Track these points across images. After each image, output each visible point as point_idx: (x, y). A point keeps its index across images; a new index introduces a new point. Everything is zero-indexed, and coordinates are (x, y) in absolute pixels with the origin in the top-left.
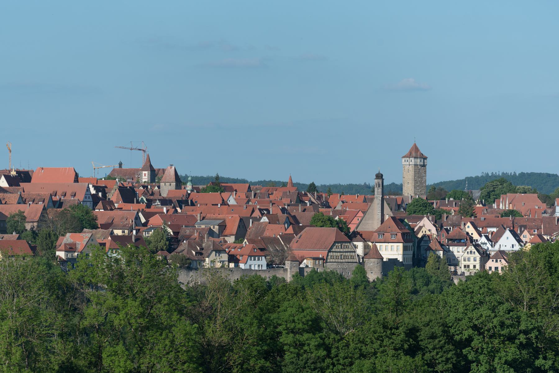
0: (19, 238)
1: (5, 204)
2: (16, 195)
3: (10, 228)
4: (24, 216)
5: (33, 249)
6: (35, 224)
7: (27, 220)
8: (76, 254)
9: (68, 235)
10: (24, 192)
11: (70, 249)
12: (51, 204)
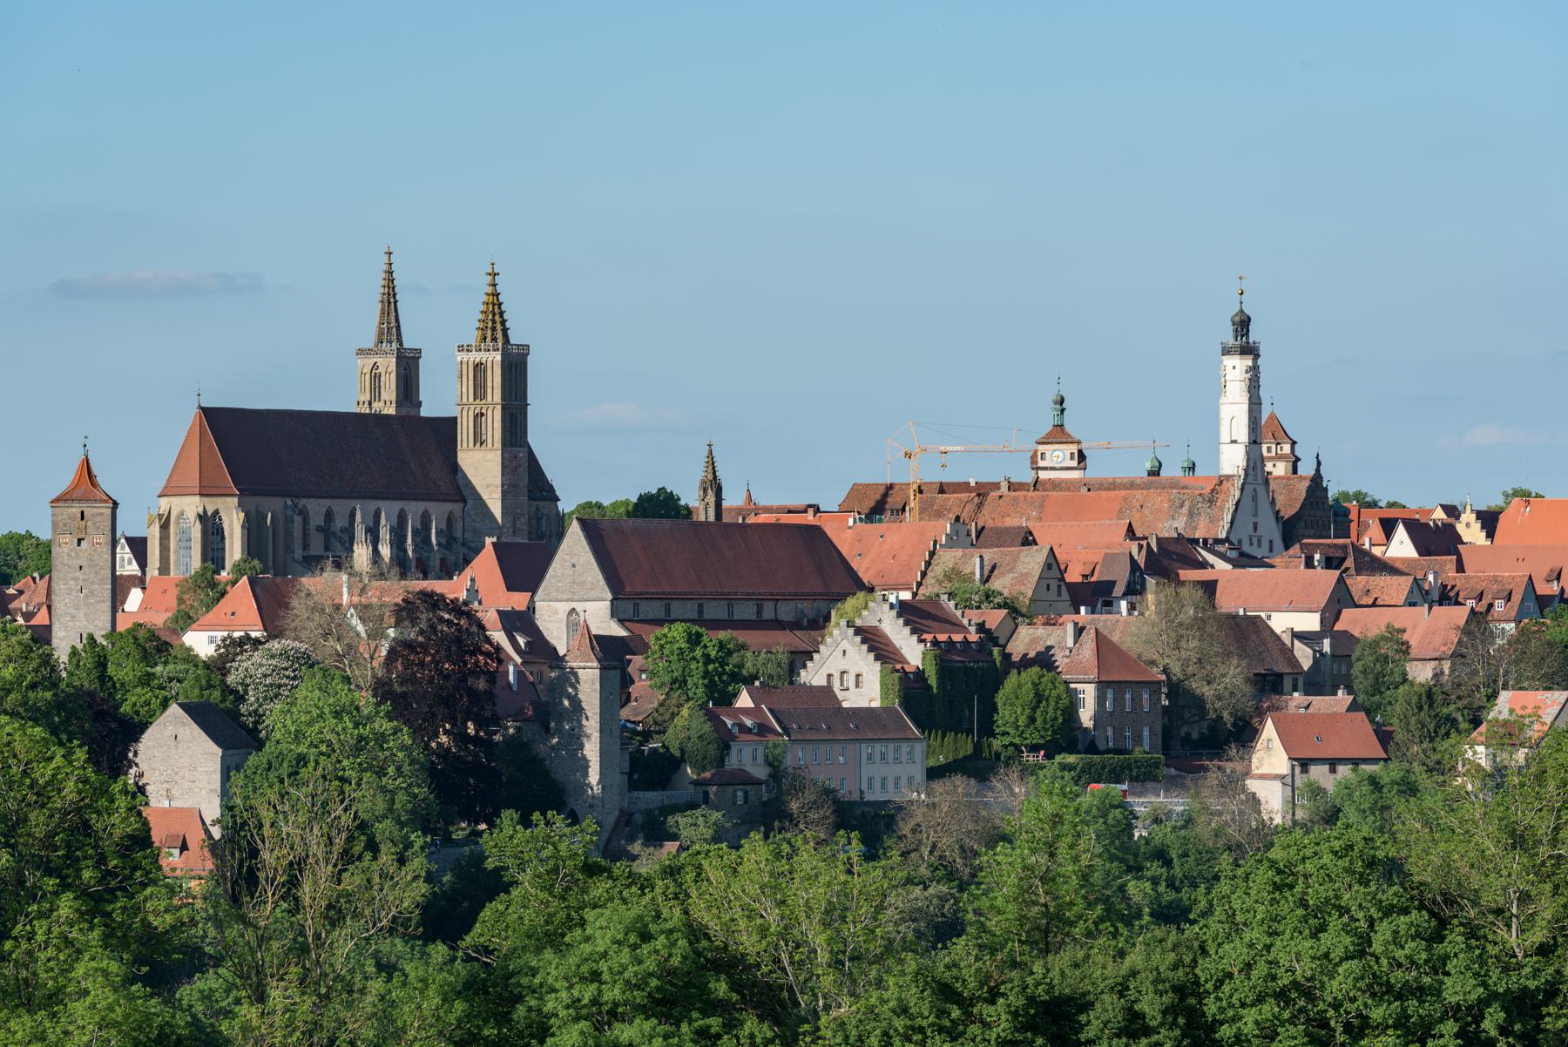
0: (1353, 707)
1: (1374, 605)
2: (1404, 578)
3: (1361, 677)
4: (1406, 643)
5: (1384, 737)
6: (1446, 666)
7: (1414, 653)
8: (1521, 755)
9: (1504, 697)
10: (1460, 568)
11: (1509, 735)
12: (1532, 605)
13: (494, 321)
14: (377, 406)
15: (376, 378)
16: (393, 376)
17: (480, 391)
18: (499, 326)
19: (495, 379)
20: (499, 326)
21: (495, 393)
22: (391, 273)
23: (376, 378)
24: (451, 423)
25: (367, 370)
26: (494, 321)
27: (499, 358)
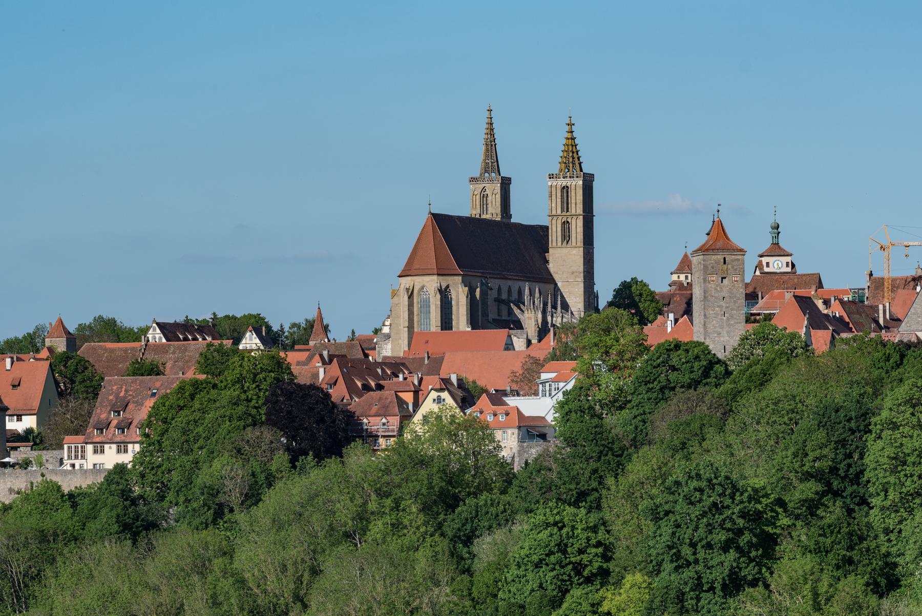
13: (572, 157)
14: (484, 217)
15: (484, 197)
16: (498, 196)
17: (566, 206)
18: (577, 162)
19: (577, 198)
20: (576, 160)
21: (577, 206)
22: (491, 124)
23: (484, 197)
24: (547, 228)
25: (477, 192)
26: (572, 157)
27: (581, 183)
